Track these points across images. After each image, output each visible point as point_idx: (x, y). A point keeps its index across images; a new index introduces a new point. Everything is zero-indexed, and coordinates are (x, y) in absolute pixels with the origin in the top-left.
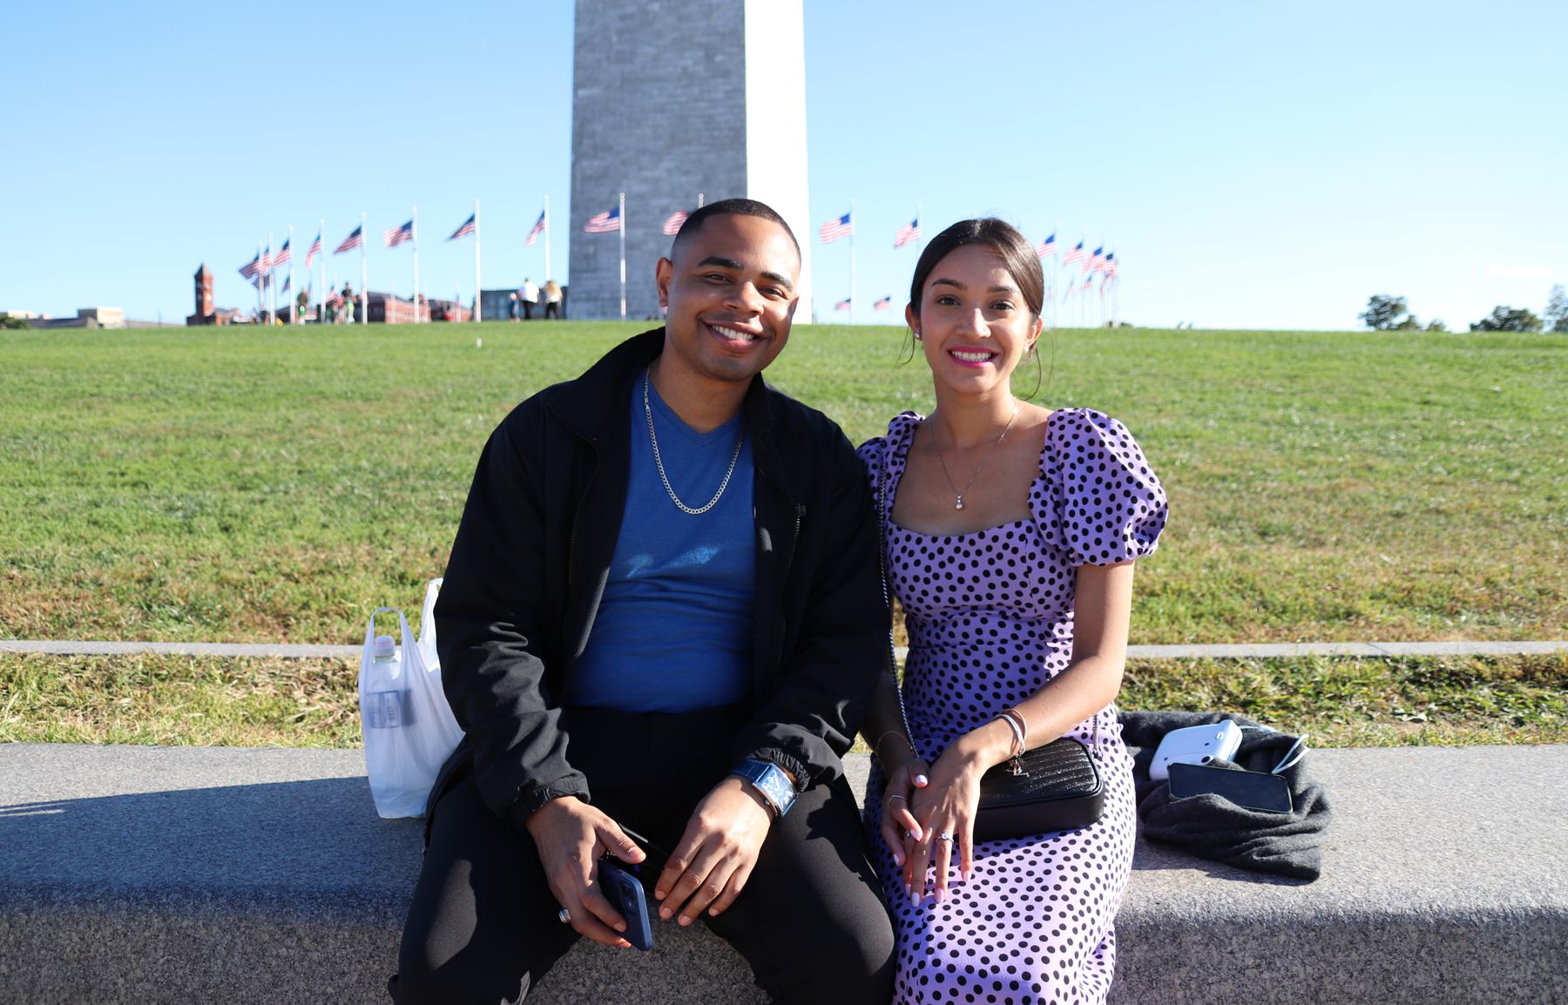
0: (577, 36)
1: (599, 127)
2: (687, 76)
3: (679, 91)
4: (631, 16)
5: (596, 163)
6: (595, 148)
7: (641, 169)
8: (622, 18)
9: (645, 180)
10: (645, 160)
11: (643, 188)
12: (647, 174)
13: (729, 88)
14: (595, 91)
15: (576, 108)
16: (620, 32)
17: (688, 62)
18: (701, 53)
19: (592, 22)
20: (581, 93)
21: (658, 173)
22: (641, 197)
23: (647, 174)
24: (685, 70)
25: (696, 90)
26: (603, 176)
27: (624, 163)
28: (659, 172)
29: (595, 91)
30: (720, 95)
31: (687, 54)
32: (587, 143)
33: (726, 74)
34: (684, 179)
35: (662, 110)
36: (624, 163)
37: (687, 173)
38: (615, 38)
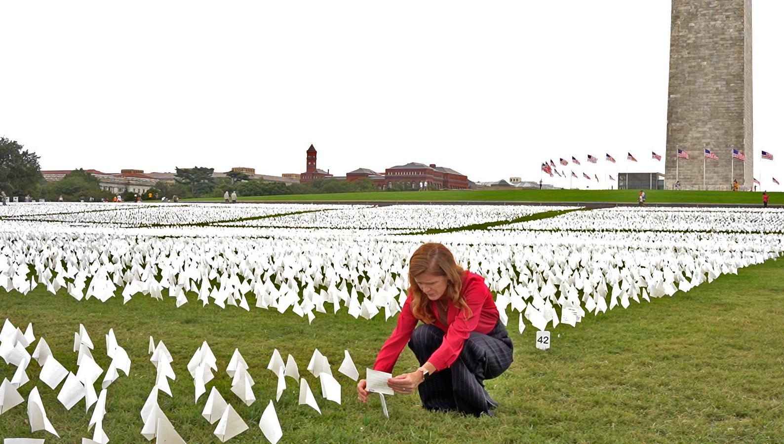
0: (670, 73)
1: (679, 110)
2: (718, 92)
3: (715, 97)
4: (694, 67)
5: (678, 124)
6: (677, 118)
7: (697, 127)
8: (690, 67)
9: (699, 132)
10: (699, 124)
11: (698, 135)
12: (699, 129)
13: (736, 97)
14: (678, 96)
15: (669, 101)
16: (689, 73)
17: (719, 86)
18: (724, 83)
19: (677, 68)
20: (671, 96)
21: (704, 129)
22: (698, 138)
23: (699, 129)
24: (717, 89)
25: (722, 97)
26: (681, 129)
27: (690, 124)
28: (706, 129)
29: (678, 96)
30: (733, 99)
31: (718, 83)
32: (673, 116)
33: (735, 91)
34: (716, 132)
35: (707, 105)
36: (690, 124)
37: (717, 129)
38: (687, 75)
